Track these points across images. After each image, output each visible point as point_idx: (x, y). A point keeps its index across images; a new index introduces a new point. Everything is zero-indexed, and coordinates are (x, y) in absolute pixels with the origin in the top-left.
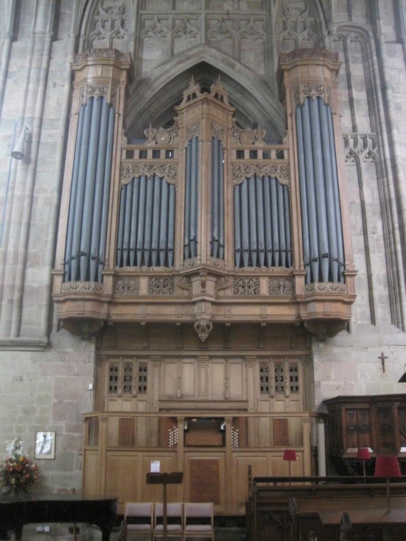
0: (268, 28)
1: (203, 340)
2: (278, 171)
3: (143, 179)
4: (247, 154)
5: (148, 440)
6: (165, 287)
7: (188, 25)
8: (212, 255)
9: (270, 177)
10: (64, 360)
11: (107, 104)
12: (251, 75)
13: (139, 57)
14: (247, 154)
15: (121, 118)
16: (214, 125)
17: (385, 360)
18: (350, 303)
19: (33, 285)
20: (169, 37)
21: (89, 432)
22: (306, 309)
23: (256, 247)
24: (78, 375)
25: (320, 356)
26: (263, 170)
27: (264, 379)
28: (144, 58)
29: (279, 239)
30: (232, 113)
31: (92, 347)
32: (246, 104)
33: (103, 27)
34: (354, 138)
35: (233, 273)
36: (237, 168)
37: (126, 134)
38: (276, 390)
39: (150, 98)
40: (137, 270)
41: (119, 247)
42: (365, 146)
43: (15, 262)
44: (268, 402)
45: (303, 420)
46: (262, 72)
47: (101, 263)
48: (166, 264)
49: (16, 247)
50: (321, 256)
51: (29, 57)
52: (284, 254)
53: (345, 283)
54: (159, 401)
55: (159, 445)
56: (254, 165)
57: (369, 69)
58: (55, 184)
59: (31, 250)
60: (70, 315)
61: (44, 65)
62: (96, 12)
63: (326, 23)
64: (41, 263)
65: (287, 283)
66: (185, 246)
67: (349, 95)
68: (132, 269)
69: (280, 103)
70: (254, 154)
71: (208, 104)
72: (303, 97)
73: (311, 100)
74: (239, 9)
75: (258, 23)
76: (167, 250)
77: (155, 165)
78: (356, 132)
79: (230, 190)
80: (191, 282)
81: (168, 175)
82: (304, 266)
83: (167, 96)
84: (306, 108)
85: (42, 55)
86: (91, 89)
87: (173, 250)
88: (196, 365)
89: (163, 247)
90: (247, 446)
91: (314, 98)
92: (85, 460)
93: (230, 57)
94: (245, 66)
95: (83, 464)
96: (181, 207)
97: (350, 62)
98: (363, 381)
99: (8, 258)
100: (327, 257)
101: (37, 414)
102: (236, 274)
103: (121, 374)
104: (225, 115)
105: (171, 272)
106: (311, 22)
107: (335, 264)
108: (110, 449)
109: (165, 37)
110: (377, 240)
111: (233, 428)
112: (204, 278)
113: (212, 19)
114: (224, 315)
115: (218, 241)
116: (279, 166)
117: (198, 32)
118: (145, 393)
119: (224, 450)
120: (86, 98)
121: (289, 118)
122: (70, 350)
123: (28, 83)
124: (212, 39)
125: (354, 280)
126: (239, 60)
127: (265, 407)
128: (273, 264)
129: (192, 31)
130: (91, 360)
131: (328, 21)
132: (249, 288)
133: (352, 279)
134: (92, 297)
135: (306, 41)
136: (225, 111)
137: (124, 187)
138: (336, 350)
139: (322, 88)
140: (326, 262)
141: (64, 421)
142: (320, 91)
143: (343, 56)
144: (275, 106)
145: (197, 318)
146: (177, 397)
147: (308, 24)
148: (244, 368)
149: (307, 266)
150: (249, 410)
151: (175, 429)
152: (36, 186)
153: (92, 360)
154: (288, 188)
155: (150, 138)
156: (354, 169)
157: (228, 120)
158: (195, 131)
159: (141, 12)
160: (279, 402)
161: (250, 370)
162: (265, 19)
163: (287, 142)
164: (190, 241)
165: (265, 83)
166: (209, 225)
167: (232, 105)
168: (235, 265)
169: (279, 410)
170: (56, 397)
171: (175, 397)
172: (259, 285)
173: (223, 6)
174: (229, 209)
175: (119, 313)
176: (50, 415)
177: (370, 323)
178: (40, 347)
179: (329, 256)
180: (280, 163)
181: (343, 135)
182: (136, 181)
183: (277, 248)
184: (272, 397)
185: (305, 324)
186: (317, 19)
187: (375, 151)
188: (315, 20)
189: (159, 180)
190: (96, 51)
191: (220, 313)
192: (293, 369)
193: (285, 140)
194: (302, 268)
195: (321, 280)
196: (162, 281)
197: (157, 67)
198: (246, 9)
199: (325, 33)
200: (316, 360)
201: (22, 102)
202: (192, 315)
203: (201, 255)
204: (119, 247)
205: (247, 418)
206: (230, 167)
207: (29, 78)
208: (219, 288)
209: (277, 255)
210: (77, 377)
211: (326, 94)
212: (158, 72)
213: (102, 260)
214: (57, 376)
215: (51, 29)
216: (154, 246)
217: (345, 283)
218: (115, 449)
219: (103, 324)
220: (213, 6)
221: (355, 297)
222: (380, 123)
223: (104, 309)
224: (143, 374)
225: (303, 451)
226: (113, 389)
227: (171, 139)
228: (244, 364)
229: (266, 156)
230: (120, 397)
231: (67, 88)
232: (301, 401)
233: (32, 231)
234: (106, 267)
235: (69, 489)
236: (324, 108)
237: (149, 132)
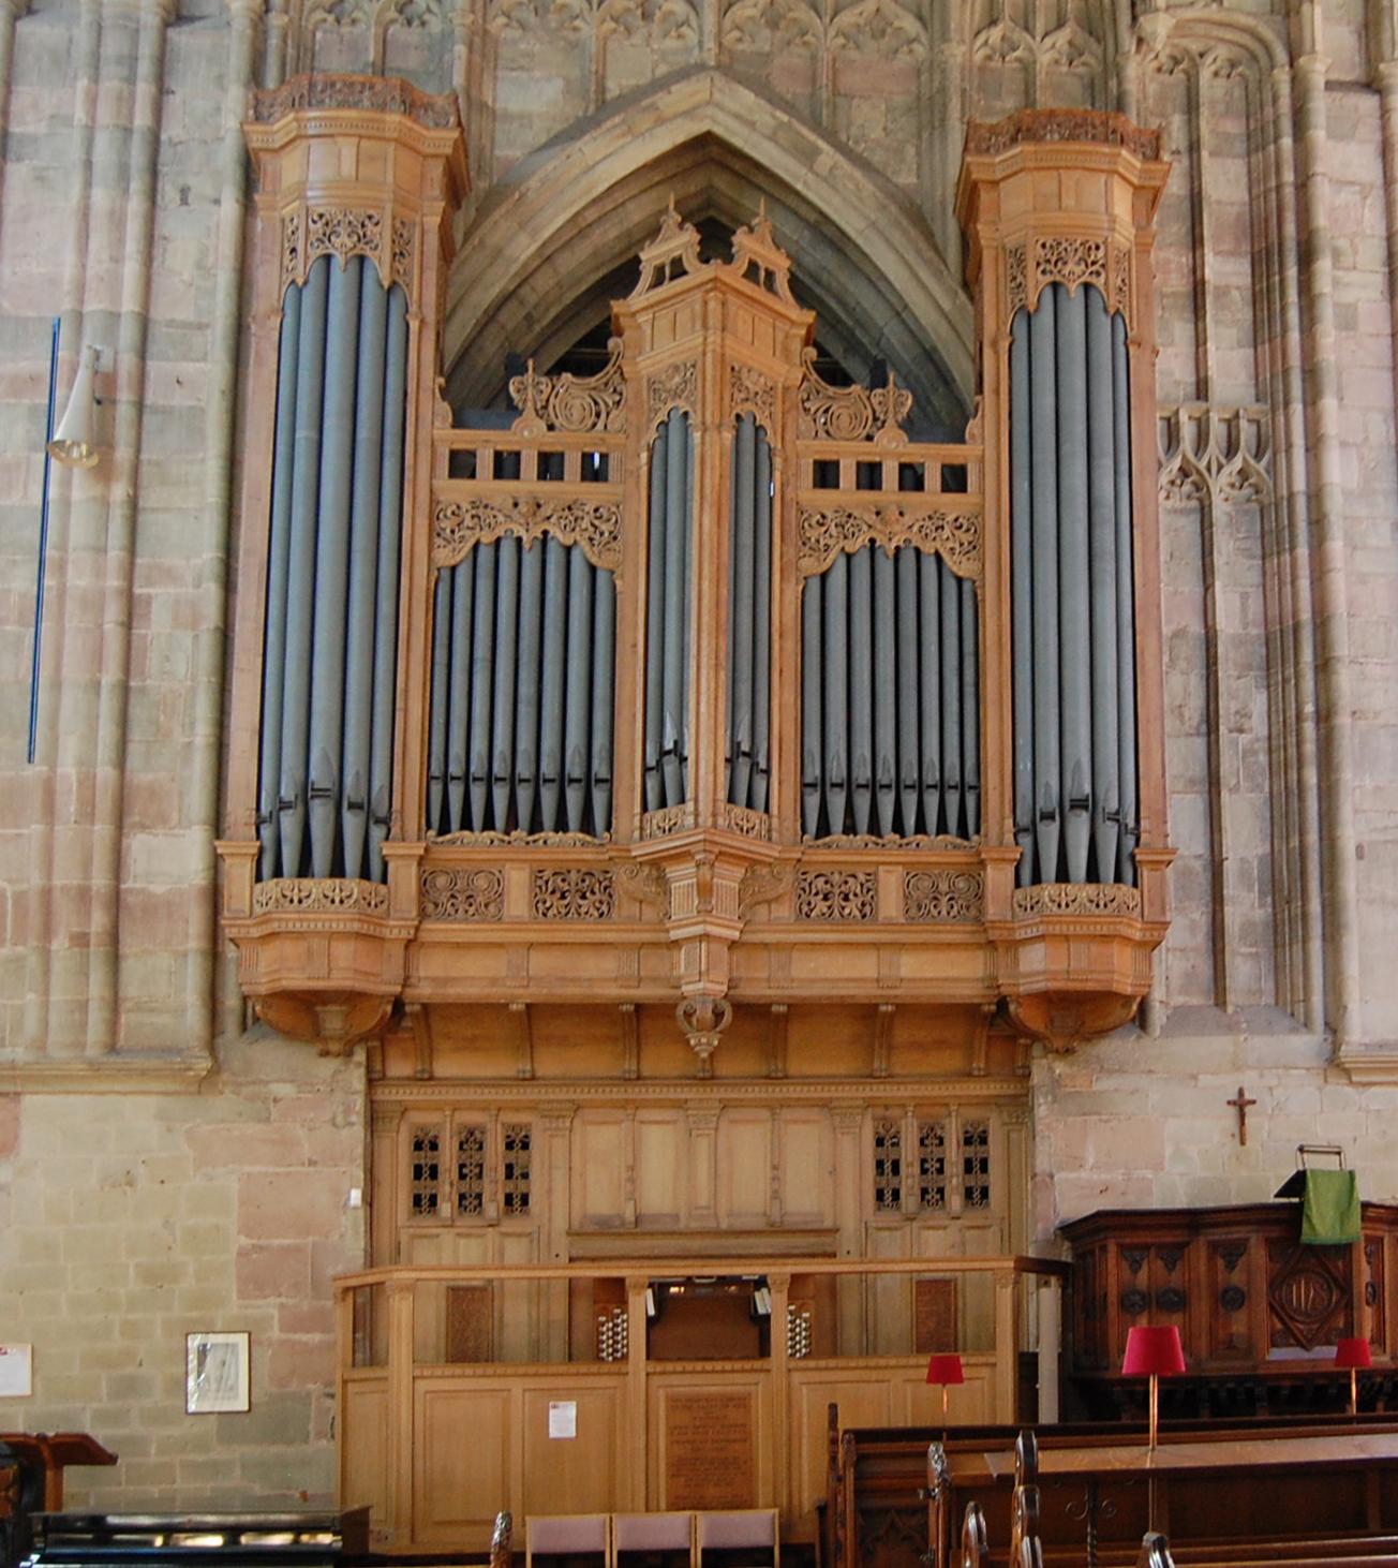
1: (704, 1055)
2: (947, 532)
4: (847, 476)
6: (584, 897)
8: (731, 799)
9: (918, 551)
14: (847, 476)
17: (1248, 1109)
26: (897, 528)
29: (936, 754)
32: (852, 288)
41: (436, 770)
43: (88, 814)
46: (906, 179)
48: (587, 826)
49: (86, 764)
51: (83, 83)
52: (953, 799)
57: (1266, 178)
59: (139, 774)
66: (646, 770)
69: (962, 296)
72: (1036, 281)
73: (1062, 291)
76: (588, 782)
79: (792, 593)
81: (591, 539)
84: (1045, 320)
86: (319, 225)
89: (575, 769)
91: (1074, 290)
92: (344, 1410)
93: (803, 121)
95: (338, 1420)
99: (60, 799)
111: (792, 1308)
116: (950, 518)
117: (692, 16)
119: (766, 1366)
120: (307, 257)
121: (987, 351)
123: (88, 184)
126: (830, 136)
132: (846, 898)
141: (272, 1300)
142: (1093, 263)
144: (946, 305)
155: (529, 412)
164: (663, 753)
165: (917, 217)
168: (804, 831)
174: (785, 653)
176: (230, 1285)
182: (485, 556)
187: (1261, 466)
189: (561, 554)
190: (333, 85)
191: (756, 975)
193: (972, 426)
196: (573, 876)
201: (69, 258)
207: (88, 164)
209: (932, 800)
213: (382, 812)
219: (389, 1009)
222: (1286, 372)
224: (517, 1156)
226: (425, 1202)
227: (598, 415)
236: (1102, 323)
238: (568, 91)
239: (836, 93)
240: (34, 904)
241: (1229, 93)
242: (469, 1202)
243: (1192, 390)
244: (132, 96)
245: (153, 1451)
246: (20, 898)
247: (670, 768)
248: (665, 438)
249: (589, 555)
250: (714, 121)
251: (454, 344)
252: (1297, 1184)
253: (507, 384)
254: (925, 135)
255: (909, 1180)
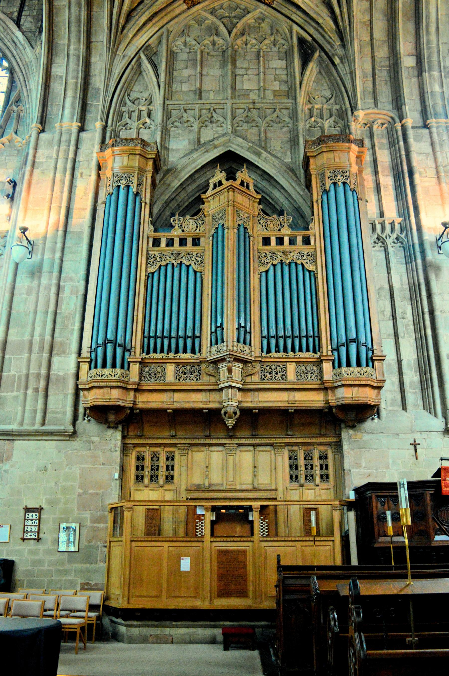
0: (294, 116)
2: (305, 257)
3: (170, 267)
4: (273, 241)
5: (175, 531)
6: (191, 374)
7: (214, 115)
8: (238, 341)
9: (296, 264)
10: (90, 449)
11: (134, 193)
12: (277, 162)
13: (165, 147)
14: (273, 241)
15: (148, 207)
16: (240, 212)
18: (380, 388)
19: (59, 374)
20: (195, 127)
21: (114, 524)
22: (334, 394)
23: (283, 333)
24: (103, 464)
25: (350, 443)
26: (289, 256)
27: (294, 467)
28: (170, 147)
30: (258, 201)
31: (119, 435)
32: (273, 192)
33: (130, 118)
34: (381, 223)
35: (260, 359)
36: (263, 255)
37: (153, 223)
38: (306, 479)
39: (176, 186)
40: (164, 357)
41: (146, 334)
42: (393, 230)
43: (41, 350)
44: (298, 491)
45: (334, 508)
46: (288, 160)
47: (128, 351)
48: (193, 352)
49: (42, 336)
50: (349, 341)
51: (56, 147)
52: (311, 340)
53: (373, 367)
54: (186, 490)
55: (187, 535)
56: (280, 251)
57: (396, 154)
58: (82, 272)
59: (57, 338)
60: (96, 403)
61: (71, 155)
62: (122, 103)
63: (352, 110)
64: (67, 351)
65: (315, 368)
66: (211, 333)
67: (376, 181)
68: (159, 356)
69: (306, 190)
70: (280, 241)
71: (234, 192)
73: (337, 186)
74: (264, 98)
75: (284, 111)
76: (194, 337)
77: (182, 253)
78: (383, 217)
79: (257, 277)
80: (218, 369)
81: (195, 263)
82: (332, 352)
83: (194, 186)
84: (332, 193)
85: (69, 146)
87: (200, 337)
88: (224, 452)
89: (189, 333)
90: (277, 536)
91: (340, 184)
92: (109, 552)
93: (256, 145)
94: (271, 154)
95: (107, 556)
96: (208, 295)
97: (377, 148)
98: (395, 468)
99: (34, 346)
100: (355, 342)
101: (61, 506)
102: (263, 360)
103: (148, 462)
104: (251, 202)
105: (198, 358)
106: (338, 110)
107: (363, 350)
108: (135, 539)
109: (192, 126)
110: (407, 325)
111: (262, 518)
112: (230, 364)
113: (238, 108)
114: (252, 402)
115: (245, 327)
116: (306, 253)
117: (225, 122)
118: (172, 482)
120: (113, 186)
121: (315, 204)
122: (96, 439)
123: (55, 173)
124: (238, 128)
125: (382, 365)
126: (266, 150)
127: (294, 495)
128: (301, 350)
129: (218, 121)
130: (117, 449)
131: (354, 108)
132: (277, 374)
133: (381, 364)
134: (119, 384)
135: (333, 128)
136: (251, 198)
137: (151, 275)
138: (366, 437)
139: (348, 174)
140: (353, 347)
141: (88, 512)
143: (370, 142)
144: (301, 193)
145: (224, 404)
146: (205, 487)
147: (334, 112)
148: (273, 456)
149: (334, 351)
150: (278, 499)
151: (202, 520)
152: (62, 275)
153: (119, 449)
154: (314, 275)
155: (177, 227)
156: (382, 255)
157: (253, 206)
158: (221, 218)
159: (167, 102)
160: (309, 491)
161: (279, 458)
162: (291, 107)
163: (313, 228)
164: (216, 327)
165: (291, 170)
166: (236, 312)
167: (258, 193)
168: (262, 351)
169: (310, 498)
170: (81, 487)
171: (202, 486)
172: (286, 370)
173: (249, 95)
174: (255, 296)
175: (145, 400)
176: (74, 506)
177: (401, 409)
178: (65, 435)
179: (356, 341)
180: (306, 249)
181: (370, 220)
182: (163, 269)
183: (304, 333)
184: (302, 486)
185: (334, 410)
186: (343, 106)
187: (403, 236)
188: (341, 107)
190: (122, 141)
192: (323, 457)
193: (311, 226)
194: (330, 353)
195: (349, 364)
196: (188, 368)
197: (183, 157)
198: (272, 98)
199: (351, 119)
200: (346, 446)
201: (49, 192)
202: (219, 402)
203: (227, 342)
204: (146, 334)
205: (276, 505)
206: (256, 253)
207: (56, 168)
208: (246, 375)
209: (304, 341)
210: (103, 466)
211: (352, 180)
212: (185, 161)
213: (128, 347)
214: (83, 466)
215: (78, 120)
216: (181, 333)
217: (373, 367)
218: (140, 539)
219: (129, 411)
220: (238, 96)
221: (384, 381)
222: (408, 208)
223: (131, 396)
224: (170, 463)
225: (333, 541)
227: (197, 227)
228: (273, 452)
229: (292, 242)
230: (147, 486)
231: (94, 177)
232: (332, 490)
233: (58, 320)
234: (133, 354)
235: (93, 583)
236: (350, 194)
237: (176, 221)
238: (190, 143)
239: (266, 138)
240: (23, 379)
241: (382, 132)
242: (154, 478)
243: (379, 215)
244: (69, 150)
245: (46, 565)
246: (19, 377)
247: (219, 332)
248: (217, 233)
249: (194, 268)
250: (232, 147)
251: (156, 210)
252: (438, 473)
253: (170, 220)
254: (293, 148)
255: (302, 471)
